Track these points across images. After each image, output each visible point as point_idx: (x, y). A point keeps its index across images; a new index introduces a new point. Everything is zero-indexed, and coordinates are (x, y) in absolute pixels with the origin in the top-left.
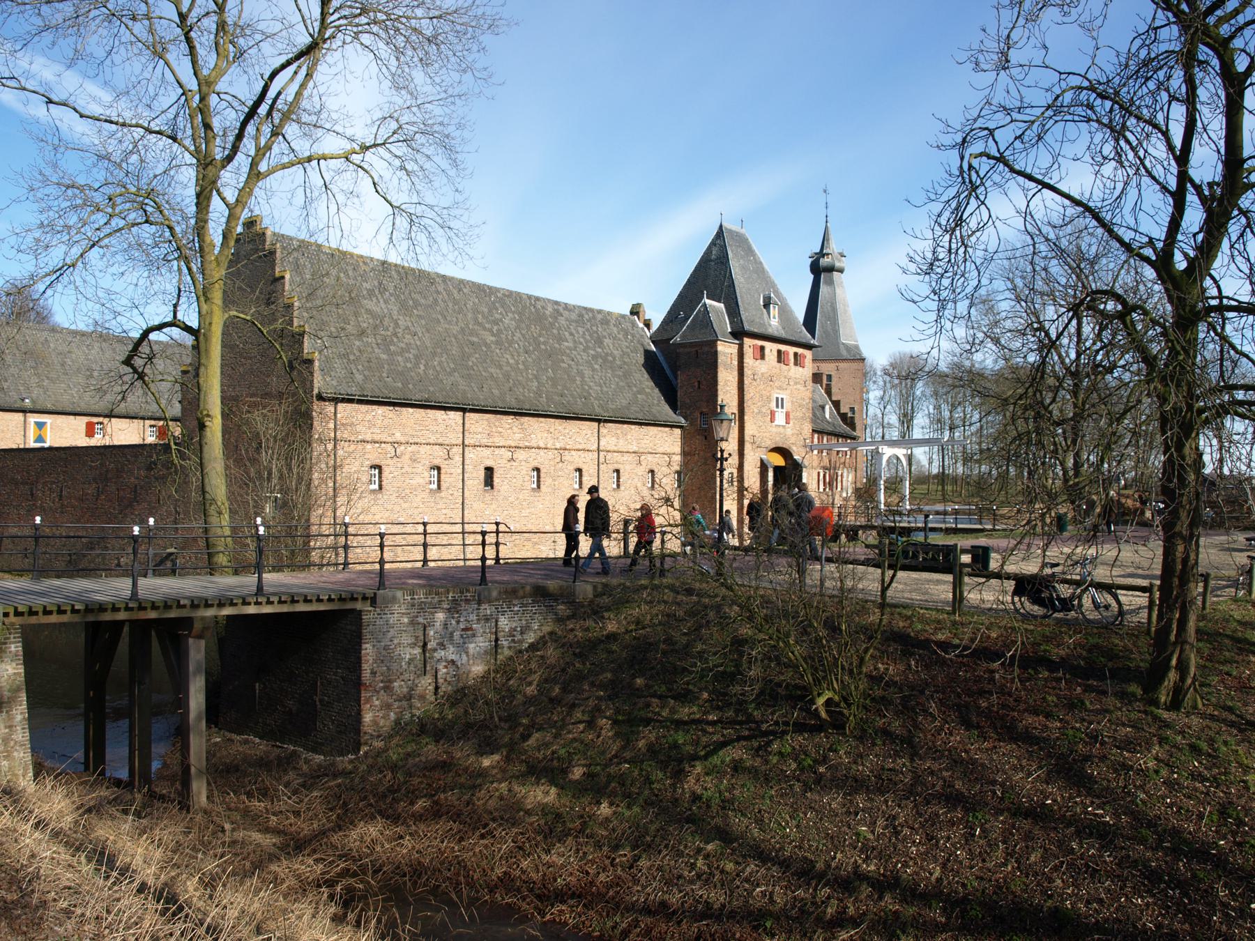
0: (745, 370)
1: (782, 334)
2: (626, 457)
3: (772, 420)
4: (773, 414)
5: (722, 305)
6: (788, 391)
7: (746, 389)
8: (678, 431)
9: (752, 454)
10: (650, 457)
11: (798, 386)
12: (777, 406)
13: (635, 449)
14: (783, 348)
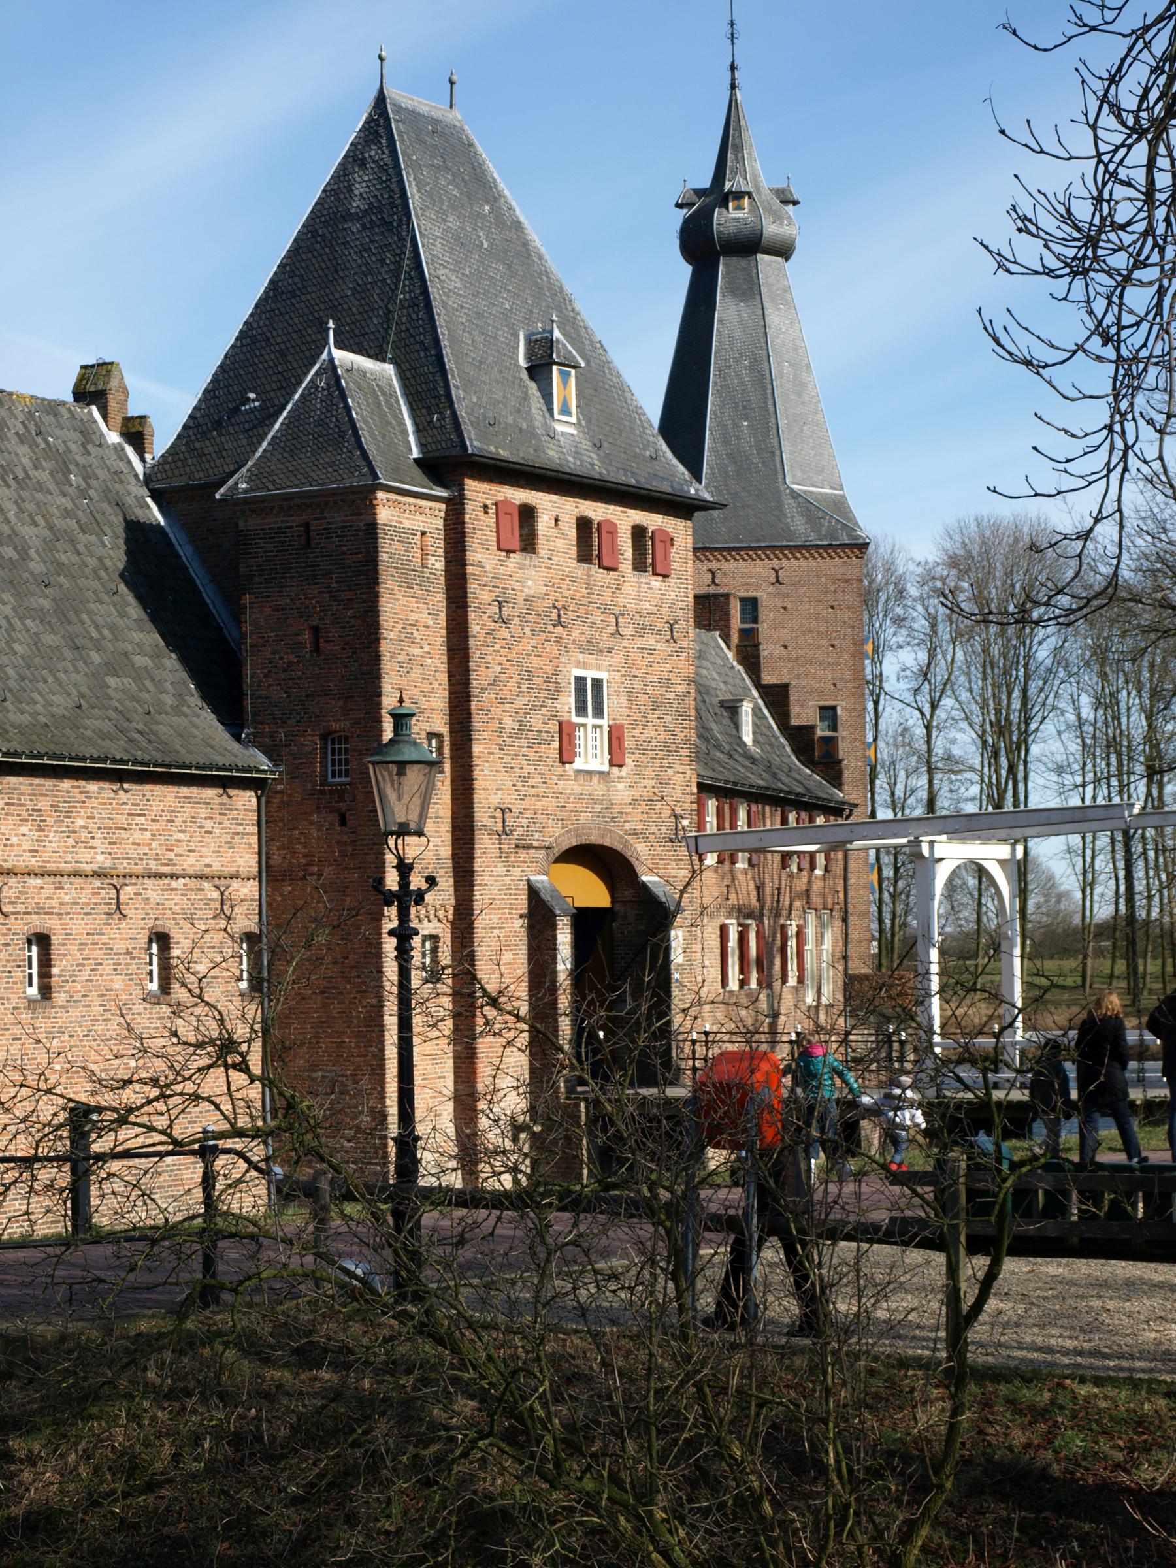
0: (472, 587)
1: (593, 464)
2: (71, 892)
3: (565, 756)
4: (566, 734)
5: (389, 369)
6: (617, 659)
7: (475, 654)
8: (247, 800)
9: (500, 869)
10: (153, 890)
11: (651, 640)
12: (581, 709)
13: (101, 861)
14: (596, 511)
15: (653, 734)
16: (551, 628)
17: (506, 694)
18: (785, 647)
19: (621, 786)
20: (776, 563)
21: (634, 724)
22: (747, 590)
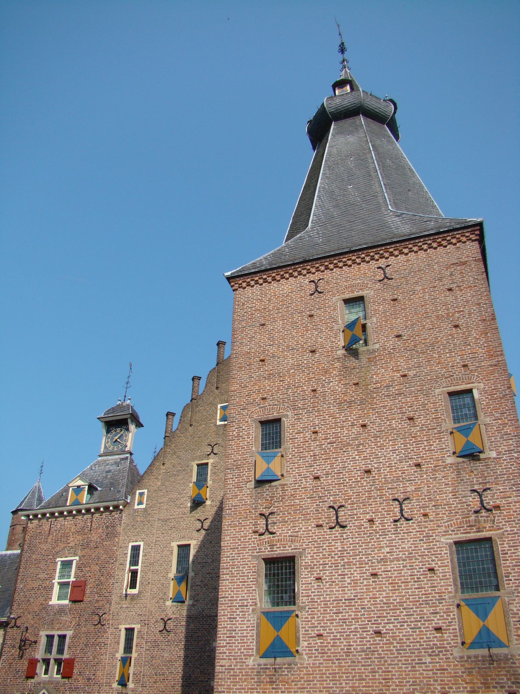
18: (398, 336)
20: (382, 263)
22: (353, 292)
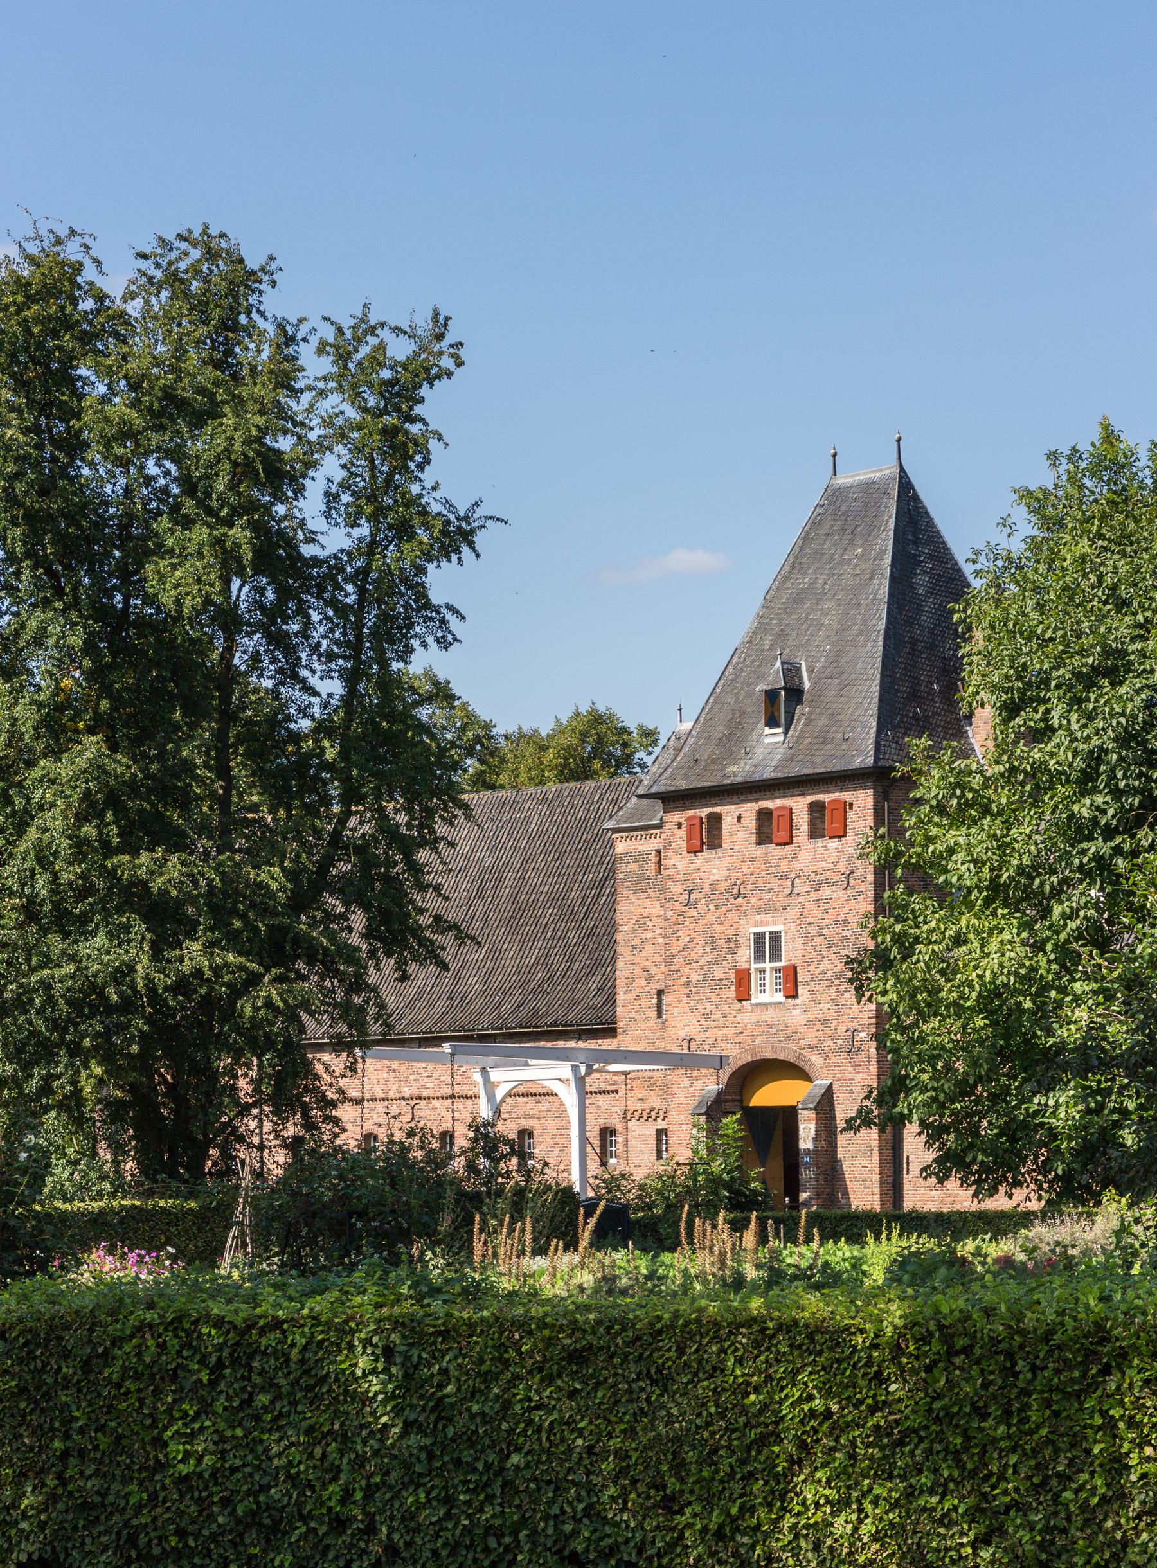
3: (743, 995)
4: (743, 981)
6: (793, 913)
11: (827, 892)
12: (759, 956)
15: (830, 966)
16: (732, 901)
17: (694, 956)
19: (795, 1012)
21: (808, 962)
